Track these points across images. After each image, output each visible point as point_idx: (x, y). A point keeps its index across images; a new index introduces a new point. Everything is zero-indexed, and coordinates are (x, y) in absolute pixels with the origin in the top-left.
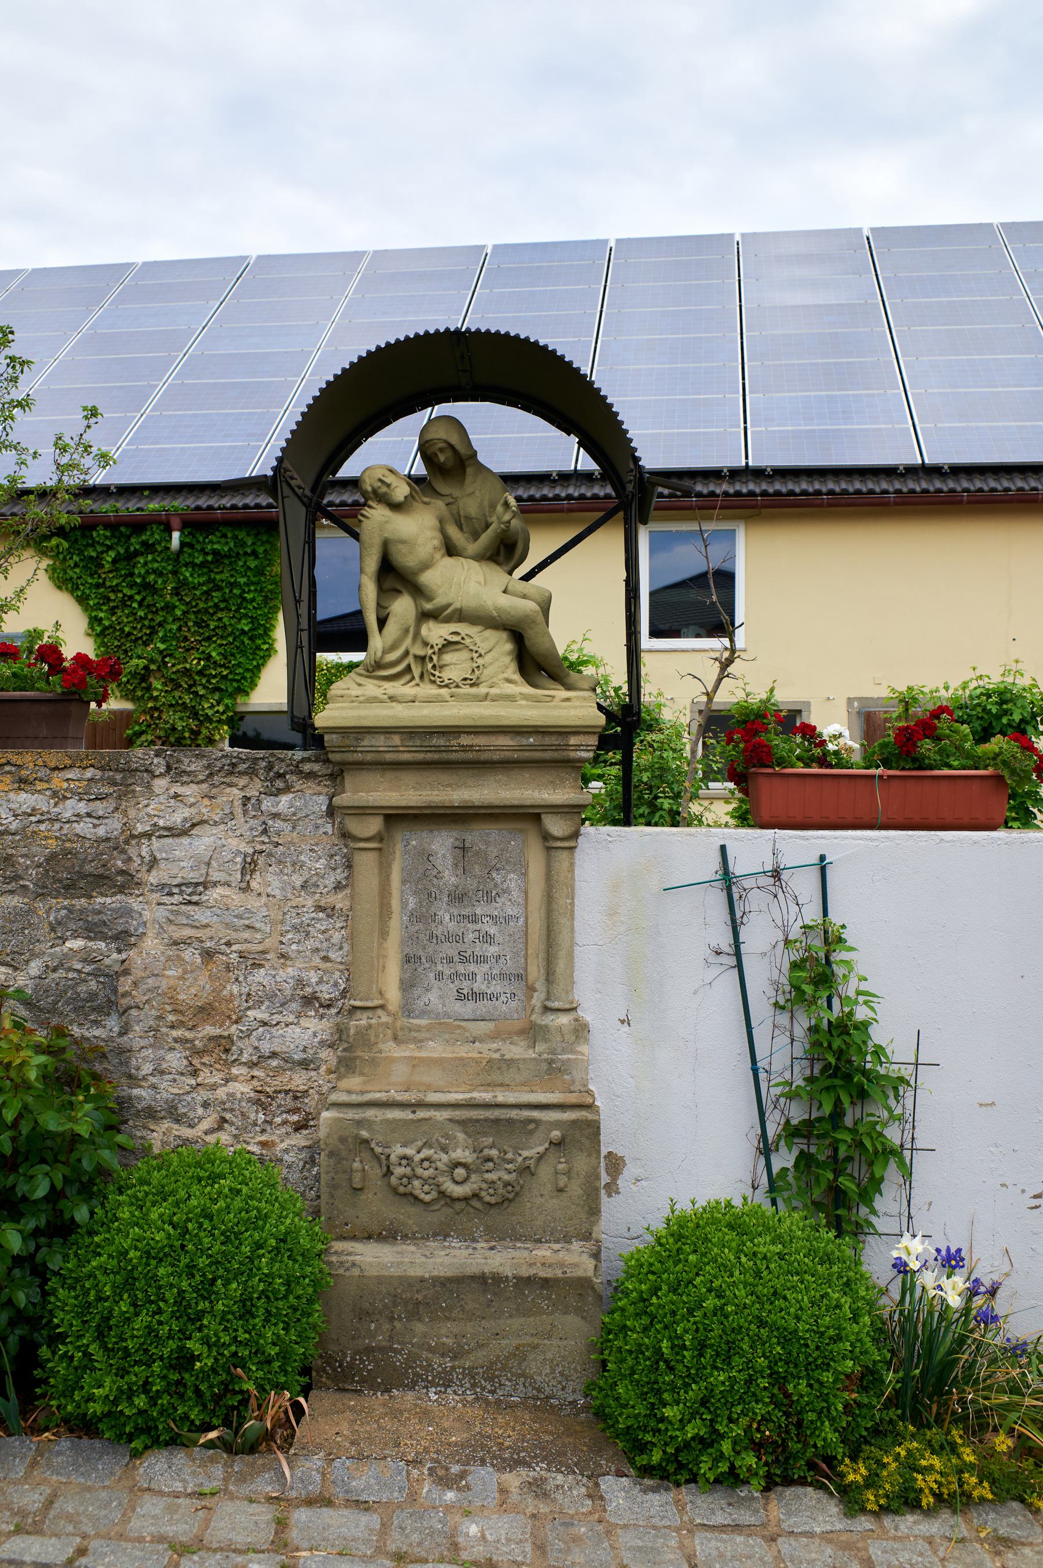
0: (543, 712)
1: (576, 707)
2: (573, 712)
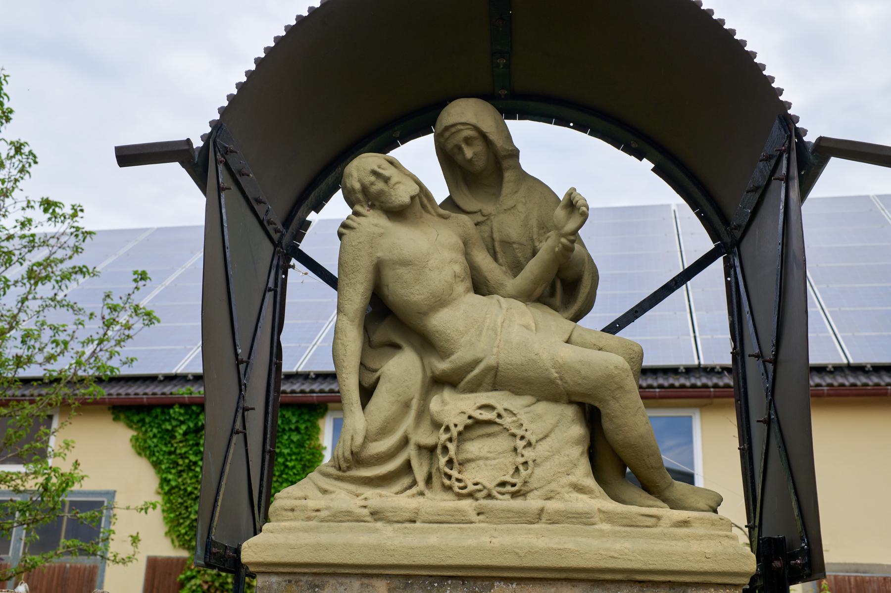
0: (642, 544)
1: (700, 538)
2: (696, 547)
